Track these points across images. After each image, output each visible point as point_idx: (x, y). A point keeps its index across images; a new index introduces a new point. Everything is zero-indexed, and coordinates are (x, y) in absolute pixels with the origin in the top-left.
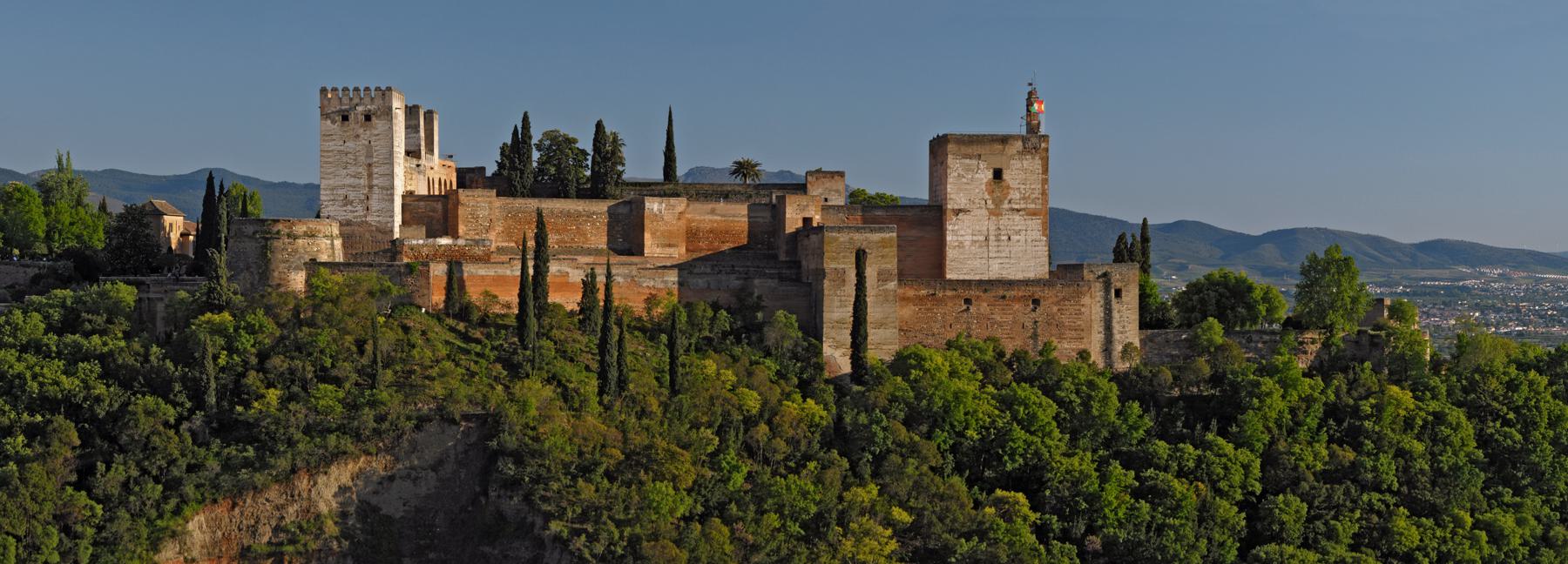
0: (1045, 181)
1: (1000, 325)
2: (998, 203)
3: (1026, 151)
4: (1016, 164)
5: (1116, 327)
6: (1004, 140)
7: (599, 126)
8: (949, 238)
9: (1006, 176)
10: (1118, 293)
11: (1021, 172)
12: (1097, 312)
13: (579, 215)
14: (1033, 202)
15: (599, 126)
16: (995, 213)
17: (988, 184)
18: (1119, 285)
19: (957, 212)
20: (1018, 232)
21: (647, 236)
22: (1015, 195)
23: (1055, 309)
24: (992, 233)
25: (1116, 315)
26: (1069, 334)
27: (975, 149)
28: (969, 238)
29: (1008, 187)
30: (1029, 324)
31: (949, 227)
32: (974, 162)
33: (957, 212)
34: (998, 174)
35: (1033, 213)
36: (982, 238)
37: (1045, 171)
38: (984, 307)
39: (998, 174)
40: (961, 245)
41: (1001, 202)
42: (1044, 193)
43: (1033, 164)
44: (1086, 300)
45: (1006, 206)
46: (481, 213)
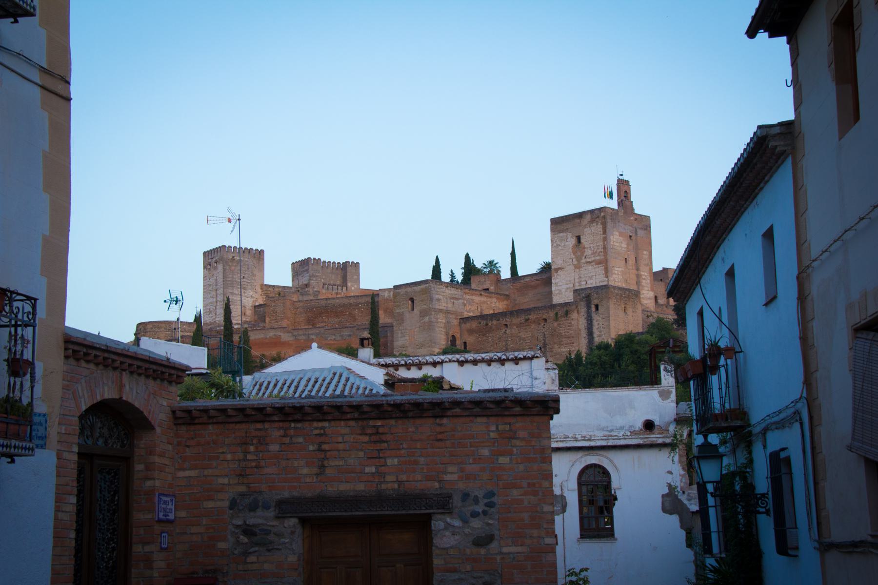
0: (605, 239)
1: (524, 339)
2: (579, 259)
3: (592, 221)
4: (587, 230)
5: (596, 333)
6: (580, 216)
7: (467, 257)
8: (553, 289)
9: (582, 241)
10: (597, 307)
11: (591, 235)
12: (582, 323)
13: (351, 305)
14: (599, 255)
15: (467, 257)
16: (578, 267)
17: (573, 247)
18: (596, 302)
19: (557, 270)
20: (591, 278)
21: (381, 312)
22: (588, 252)
23: (556, 324)
24: (577, 281)
25: (595, 323)
26: (565, 341)
27: (565, 225)
28: (564, 287)
29: (584, 248)
30: (541, 338)
31: (553, 281)
32: (565, 234)
33: (557, 270)
34: (579, 238)
35: (599, 263)
36: (571, 286)
37: (604, 232)
38: (514, 330)
39: (579, 238)
40: (560, 293)
41: (581, 259)
42: (605, 248)
43: (597, 228)
44: (574, 315)
45: (584, 261)
46: (278, 310)
